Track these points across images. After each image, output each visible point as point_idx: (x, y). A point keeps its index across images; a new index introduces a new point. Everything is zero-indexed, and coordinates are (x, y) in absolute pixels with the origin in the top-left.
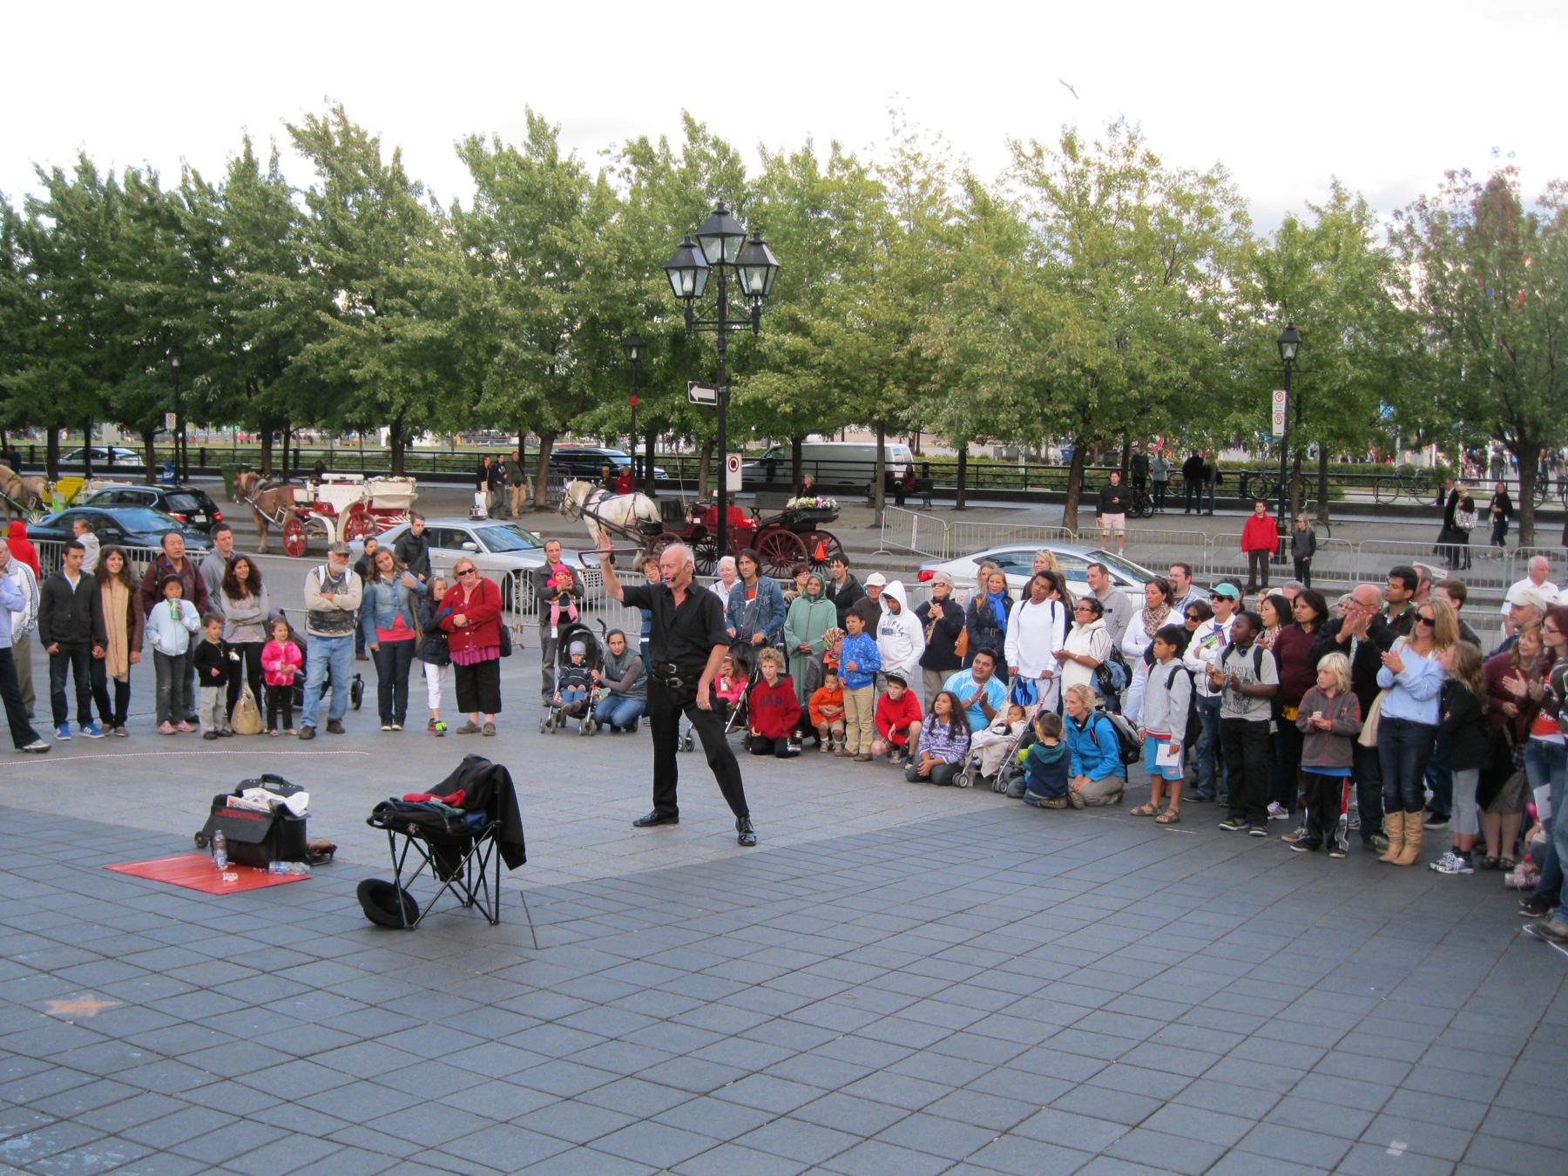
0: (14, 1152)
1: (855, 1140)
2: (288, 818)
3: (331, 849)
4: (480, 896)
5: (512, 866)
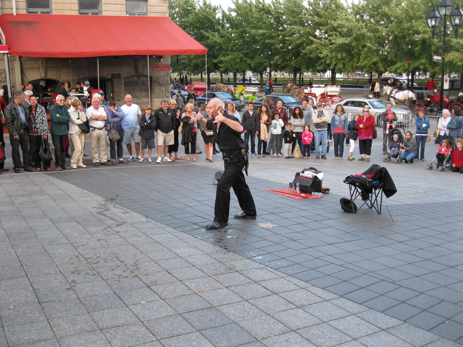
0: (259, 259)
2: (317, 180)
3: (328, 190)
4: (375, 205)
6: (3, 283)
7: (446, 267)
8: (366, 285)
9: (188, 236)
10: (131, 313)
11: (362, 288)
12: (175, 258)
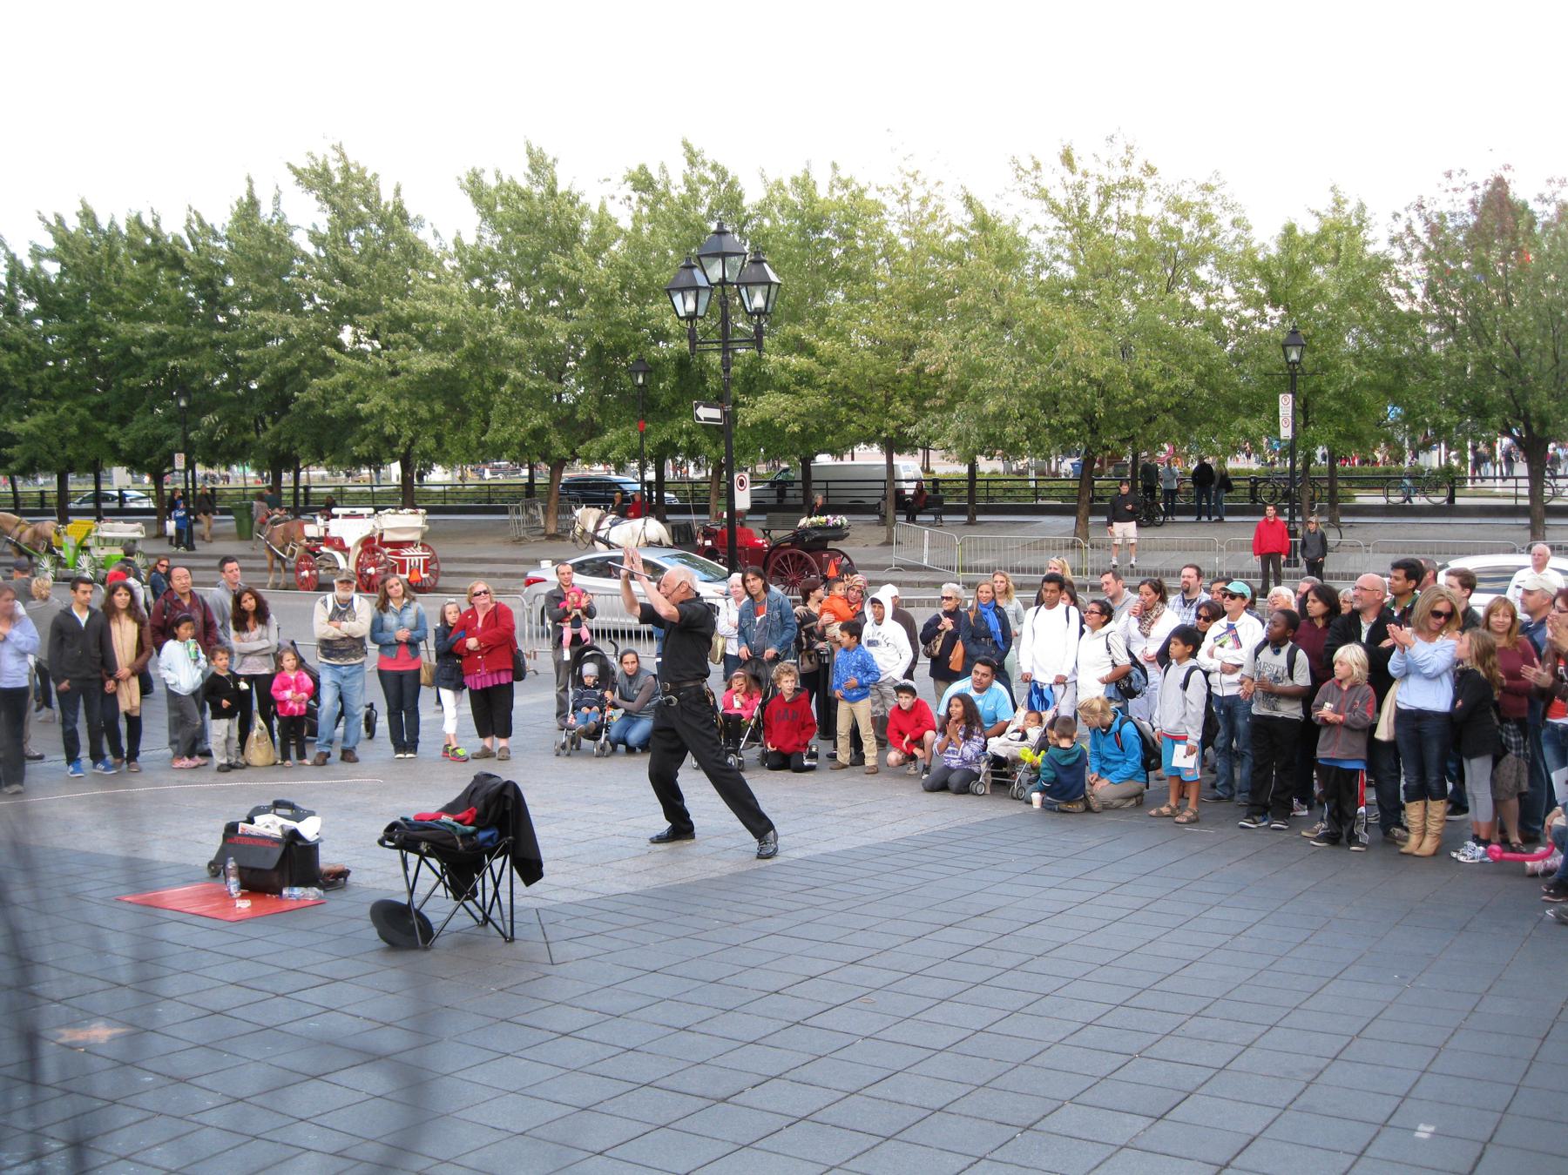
1: (875, 1140)
2: (300, 843)
3: (344, 874)
5: (528, 883)
7: (702, 1103)
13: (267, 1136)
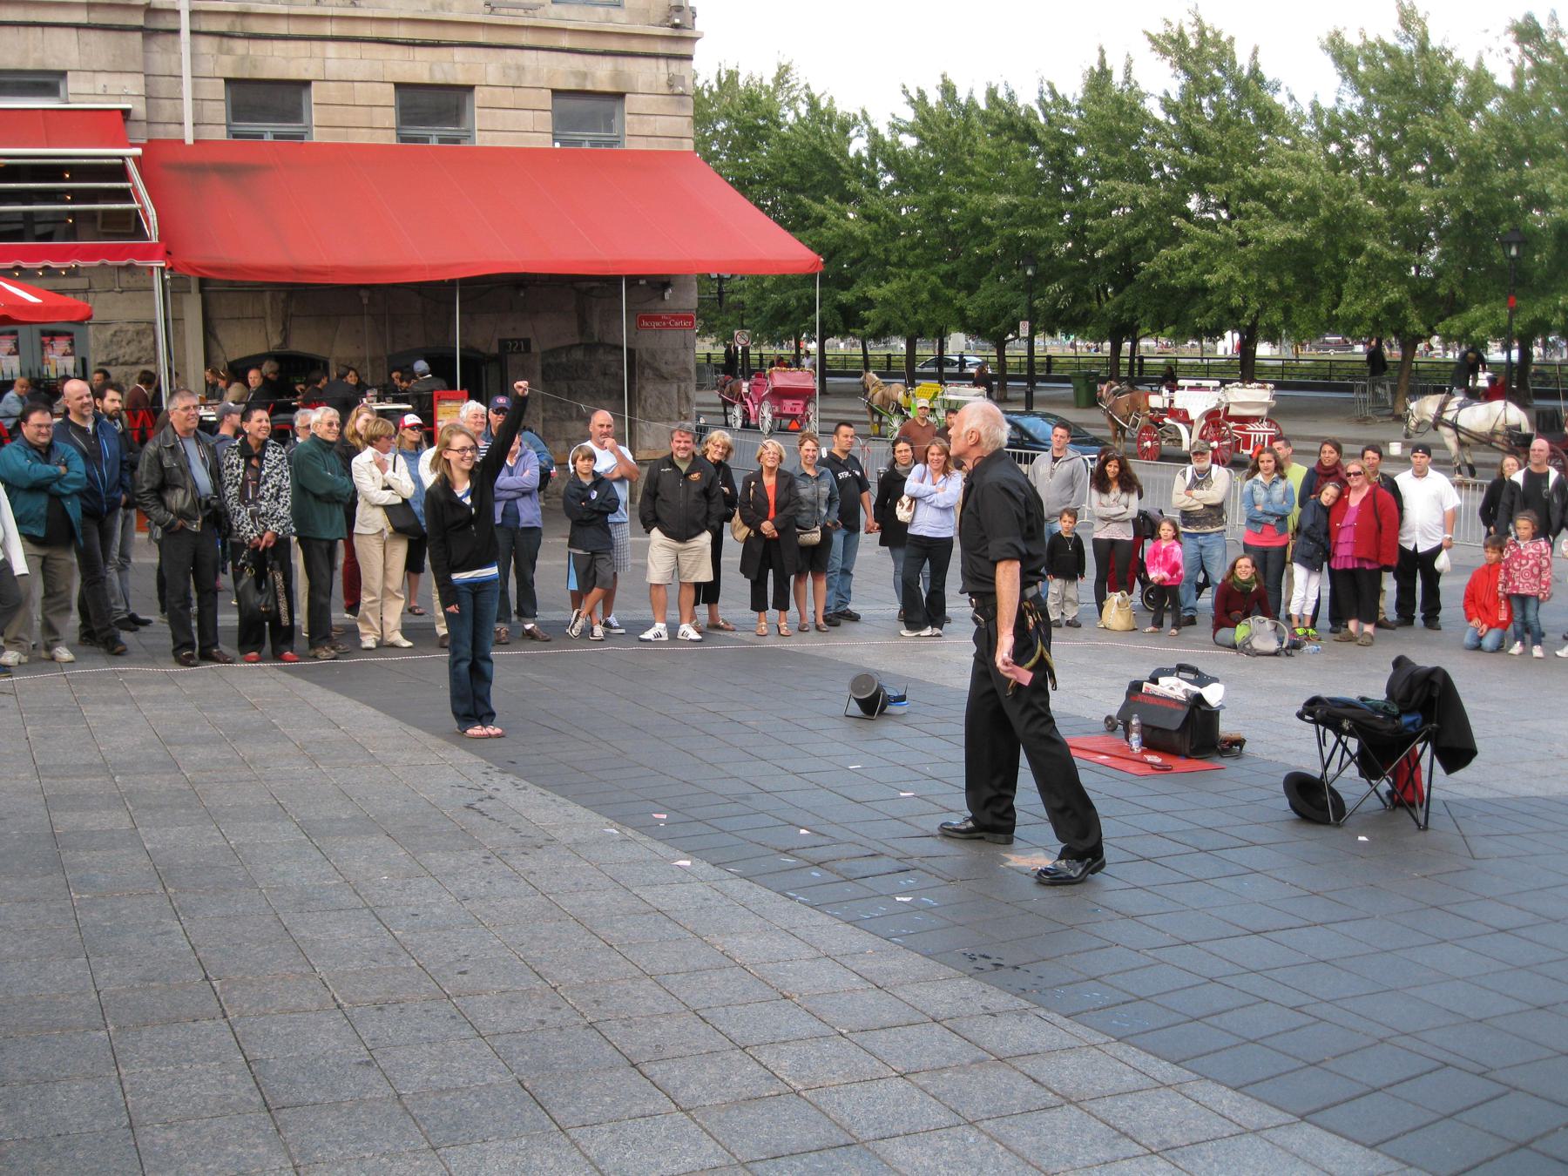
2: (1203, 708)
3: (1240, 742)
6: (145, 1034)
8: (1387, 1082)
9: (764, 892)
10: (576, 1155)
11: (1376, 1091)
12: (721, 968)
13: (1225, 980)
